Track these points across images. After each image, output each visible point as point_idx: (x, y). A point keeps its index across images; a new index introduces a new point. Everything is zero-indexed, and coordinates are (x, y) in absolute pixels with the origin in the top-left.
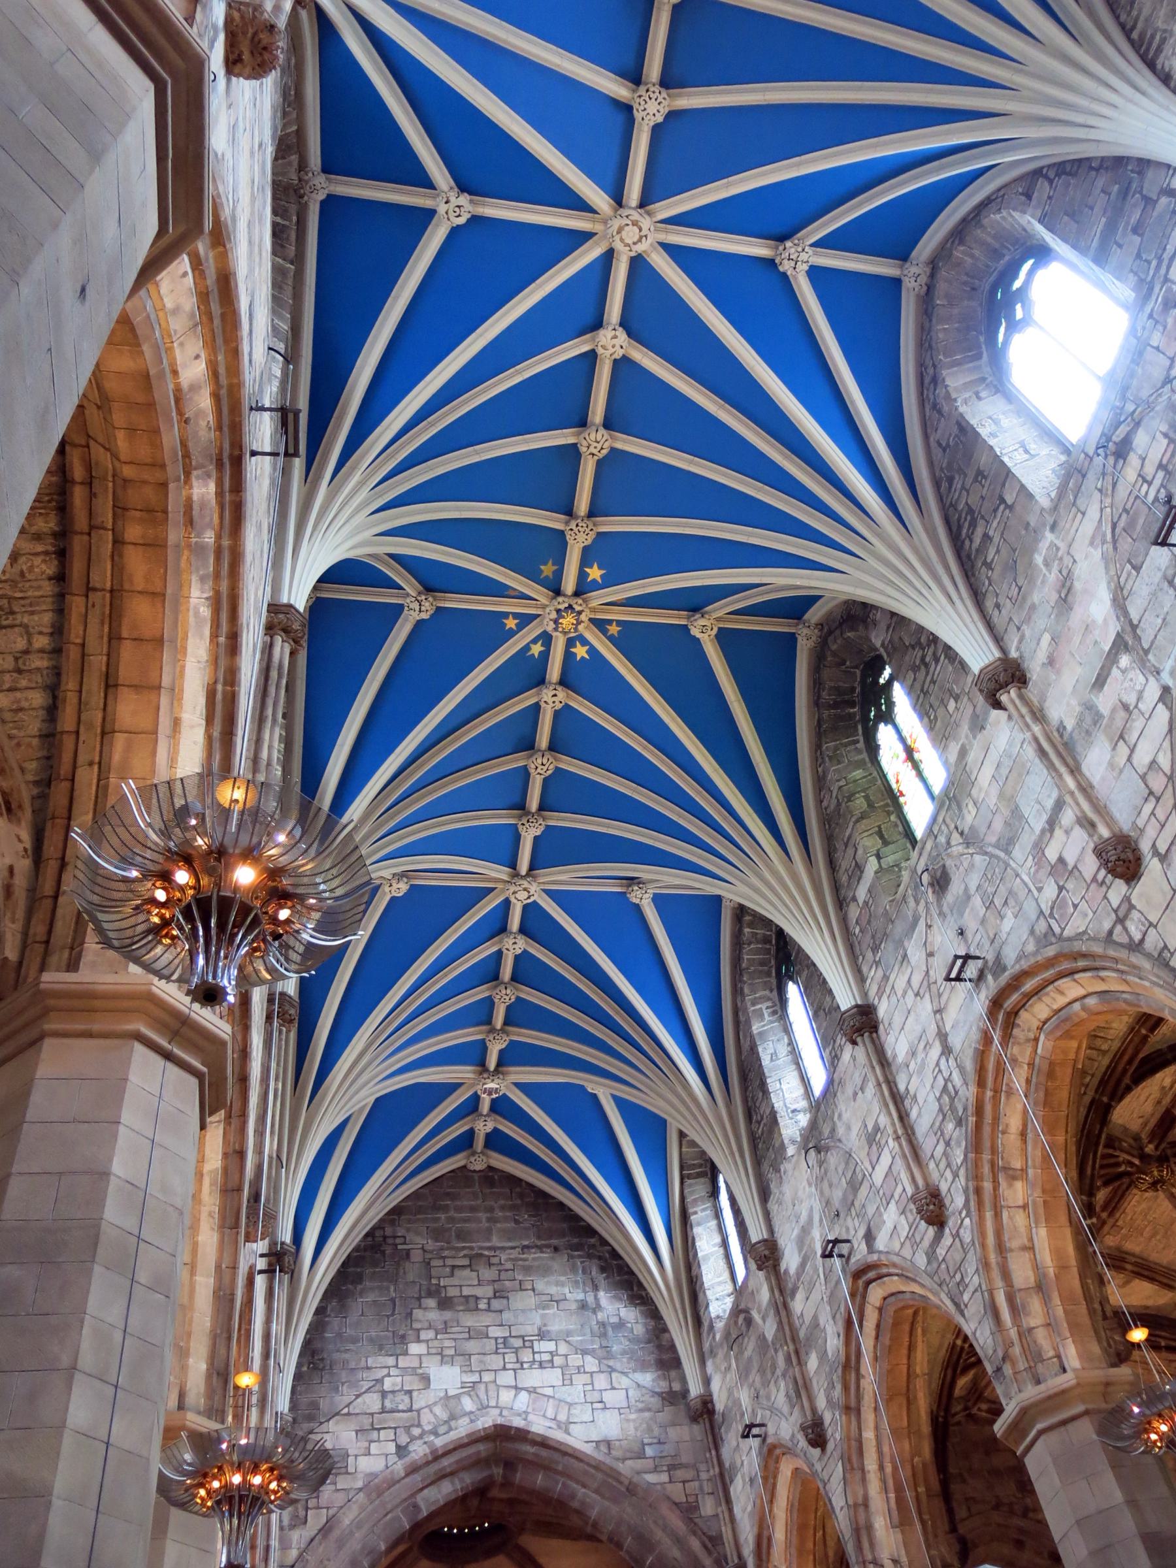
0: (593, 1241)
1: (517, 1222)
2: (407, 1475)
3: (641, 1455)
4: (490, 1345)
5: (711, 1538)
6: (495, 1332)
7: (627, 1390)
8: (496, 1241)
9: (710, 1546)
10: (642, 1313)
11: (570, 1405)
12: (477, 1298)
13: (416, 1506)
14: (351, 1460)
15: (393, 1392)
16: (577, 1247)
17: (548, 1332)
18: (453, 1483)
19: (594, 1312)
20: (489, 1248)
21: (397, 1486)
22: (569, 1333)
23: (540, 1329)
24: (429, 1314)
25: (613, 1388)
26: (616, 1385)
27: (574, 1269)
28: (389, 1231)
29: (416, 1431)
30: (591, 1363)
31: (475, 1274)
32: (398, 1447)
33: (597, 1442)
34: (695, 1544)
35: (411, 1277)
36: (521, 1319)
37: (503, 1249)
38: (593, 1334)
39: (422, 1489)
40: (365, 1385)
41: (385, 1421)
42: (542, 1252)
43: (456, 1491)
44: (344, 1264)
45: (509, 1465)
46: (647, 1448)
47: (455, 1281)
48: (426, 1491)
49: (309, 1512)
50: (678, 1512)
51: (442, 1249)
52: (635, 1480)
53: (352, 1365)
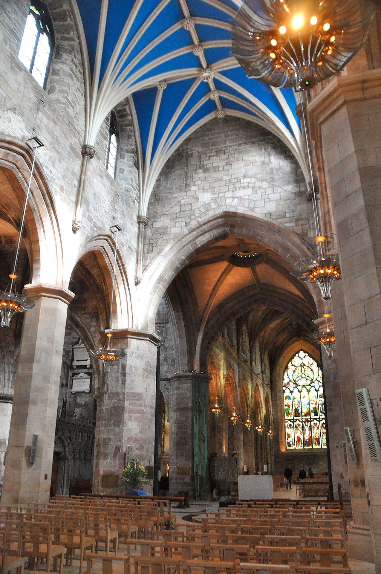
0: (270, 137)
1: (237, 135)
2: (190, 233)
3: (284, 217)
4: (223, 183)
5: (311, 246)
6: (225, 178)
7: (280, 193)
8: (228, 144)
9: (310, 248)
10: (290, 162)
11: (255, 201)
12: (219, 167)
13: (195, 243)
14: (168, 229)
15: (184, 205)
16: (264, 140)
17: (248, 175)
18: (210, 234)
19: (268, 164)
20: (224, 147)
21: (187, 237)
22: (257, 174)
23: (244, 174)
24: (200, 174)
25: (274, 193)
26: (275, 191)
27: (260, 149)
28: (185, 147)
29: (193, 217)
30: (265, 185)
31: (218, 157)
32: (186, 223)
33: (265, 214)
34: (304, 248)
35: (192, 163)
36: (237, 171)
37: (231, 146)
38: (267, 173)
39: (197, 237)
40: (174, 204)
41: (181, 215)
42: (247, 145)
43: (211, 237)
44: (167, 162)
45: (232, 226)
46: (287, 214)
47: (210, 161)
48: (199, 238)
49: (154, 248)
50: (298, 237)
51: (206, 150)
52: (280, 226)
53: (170, 197)
